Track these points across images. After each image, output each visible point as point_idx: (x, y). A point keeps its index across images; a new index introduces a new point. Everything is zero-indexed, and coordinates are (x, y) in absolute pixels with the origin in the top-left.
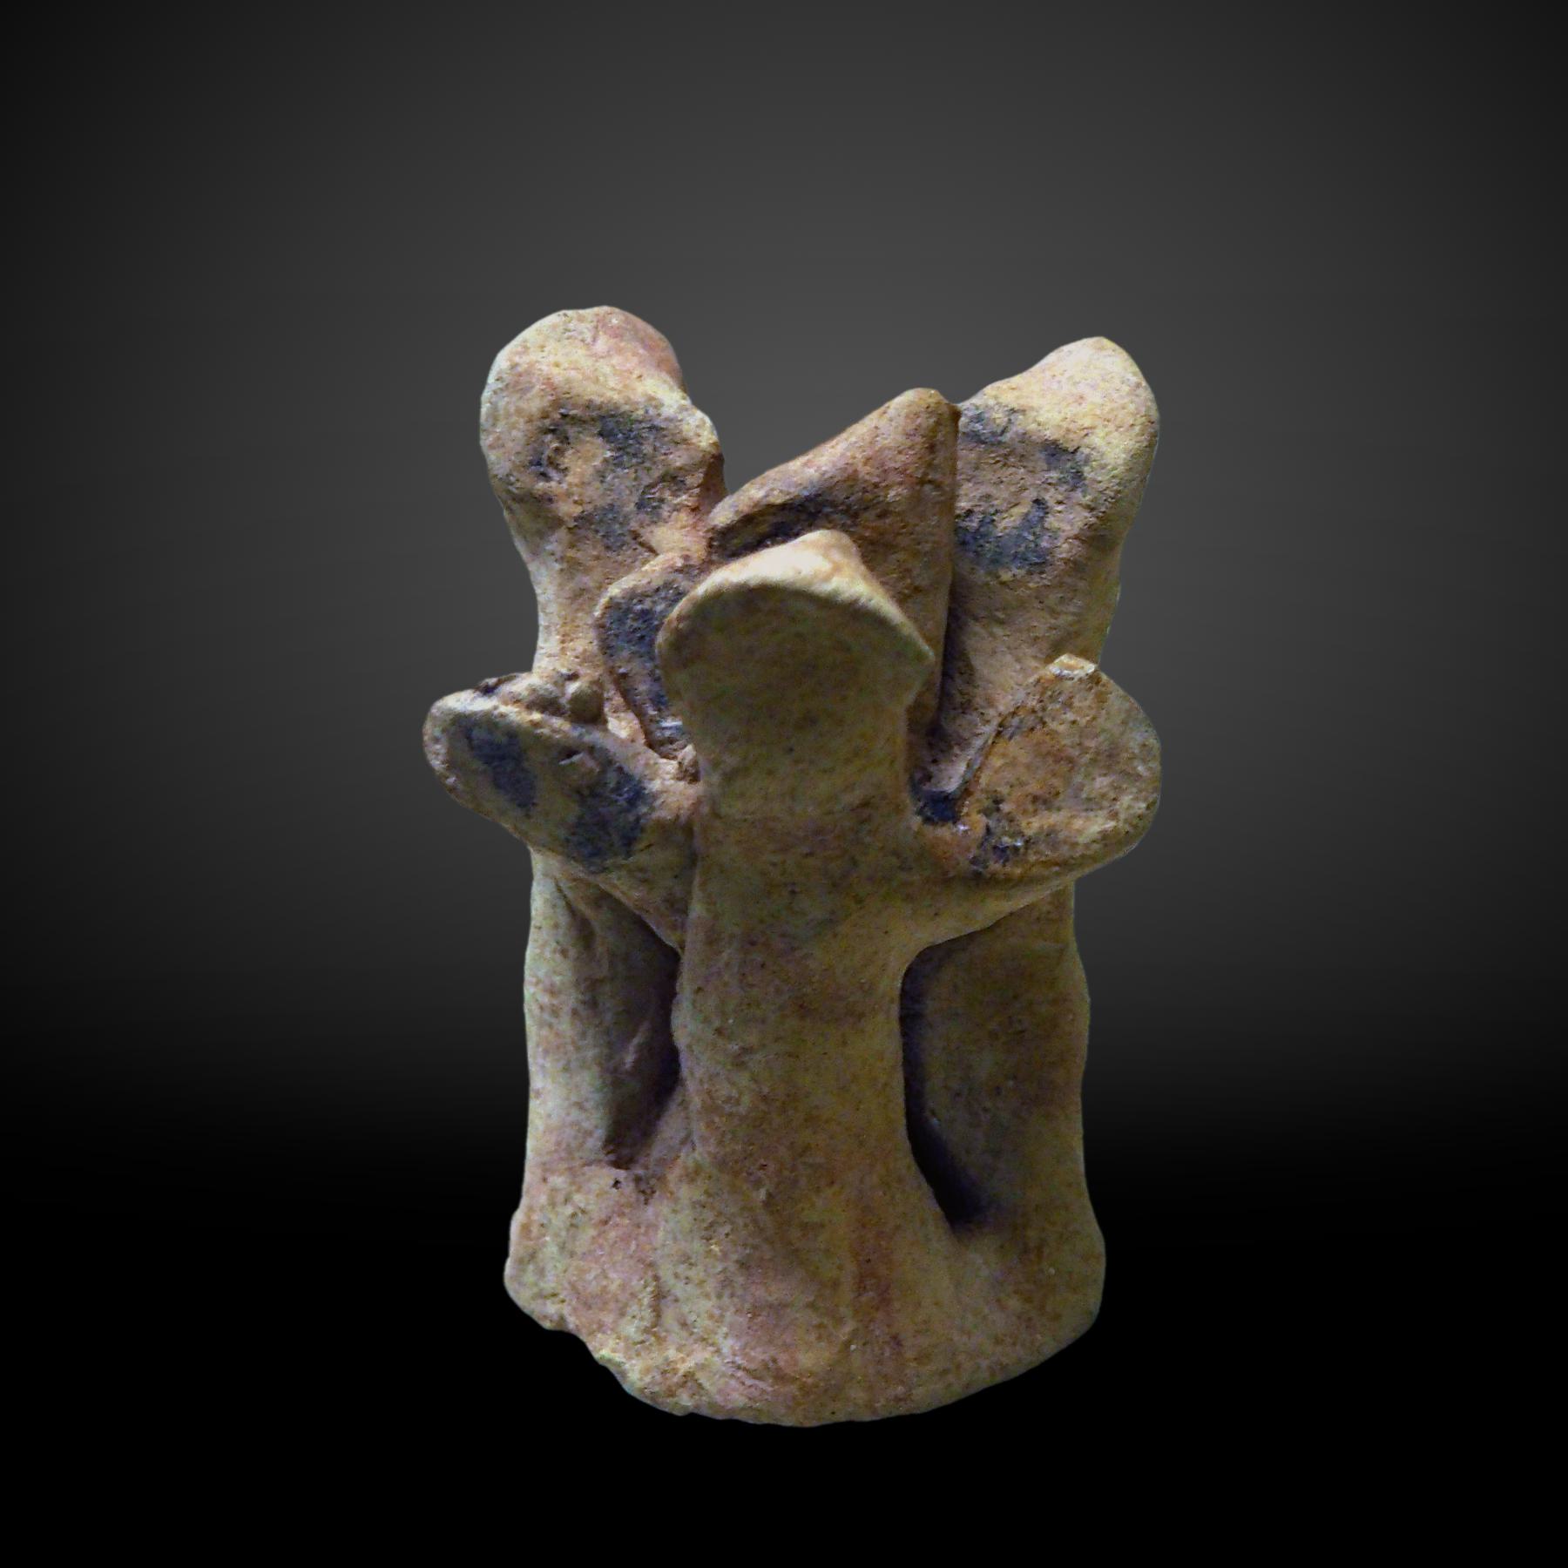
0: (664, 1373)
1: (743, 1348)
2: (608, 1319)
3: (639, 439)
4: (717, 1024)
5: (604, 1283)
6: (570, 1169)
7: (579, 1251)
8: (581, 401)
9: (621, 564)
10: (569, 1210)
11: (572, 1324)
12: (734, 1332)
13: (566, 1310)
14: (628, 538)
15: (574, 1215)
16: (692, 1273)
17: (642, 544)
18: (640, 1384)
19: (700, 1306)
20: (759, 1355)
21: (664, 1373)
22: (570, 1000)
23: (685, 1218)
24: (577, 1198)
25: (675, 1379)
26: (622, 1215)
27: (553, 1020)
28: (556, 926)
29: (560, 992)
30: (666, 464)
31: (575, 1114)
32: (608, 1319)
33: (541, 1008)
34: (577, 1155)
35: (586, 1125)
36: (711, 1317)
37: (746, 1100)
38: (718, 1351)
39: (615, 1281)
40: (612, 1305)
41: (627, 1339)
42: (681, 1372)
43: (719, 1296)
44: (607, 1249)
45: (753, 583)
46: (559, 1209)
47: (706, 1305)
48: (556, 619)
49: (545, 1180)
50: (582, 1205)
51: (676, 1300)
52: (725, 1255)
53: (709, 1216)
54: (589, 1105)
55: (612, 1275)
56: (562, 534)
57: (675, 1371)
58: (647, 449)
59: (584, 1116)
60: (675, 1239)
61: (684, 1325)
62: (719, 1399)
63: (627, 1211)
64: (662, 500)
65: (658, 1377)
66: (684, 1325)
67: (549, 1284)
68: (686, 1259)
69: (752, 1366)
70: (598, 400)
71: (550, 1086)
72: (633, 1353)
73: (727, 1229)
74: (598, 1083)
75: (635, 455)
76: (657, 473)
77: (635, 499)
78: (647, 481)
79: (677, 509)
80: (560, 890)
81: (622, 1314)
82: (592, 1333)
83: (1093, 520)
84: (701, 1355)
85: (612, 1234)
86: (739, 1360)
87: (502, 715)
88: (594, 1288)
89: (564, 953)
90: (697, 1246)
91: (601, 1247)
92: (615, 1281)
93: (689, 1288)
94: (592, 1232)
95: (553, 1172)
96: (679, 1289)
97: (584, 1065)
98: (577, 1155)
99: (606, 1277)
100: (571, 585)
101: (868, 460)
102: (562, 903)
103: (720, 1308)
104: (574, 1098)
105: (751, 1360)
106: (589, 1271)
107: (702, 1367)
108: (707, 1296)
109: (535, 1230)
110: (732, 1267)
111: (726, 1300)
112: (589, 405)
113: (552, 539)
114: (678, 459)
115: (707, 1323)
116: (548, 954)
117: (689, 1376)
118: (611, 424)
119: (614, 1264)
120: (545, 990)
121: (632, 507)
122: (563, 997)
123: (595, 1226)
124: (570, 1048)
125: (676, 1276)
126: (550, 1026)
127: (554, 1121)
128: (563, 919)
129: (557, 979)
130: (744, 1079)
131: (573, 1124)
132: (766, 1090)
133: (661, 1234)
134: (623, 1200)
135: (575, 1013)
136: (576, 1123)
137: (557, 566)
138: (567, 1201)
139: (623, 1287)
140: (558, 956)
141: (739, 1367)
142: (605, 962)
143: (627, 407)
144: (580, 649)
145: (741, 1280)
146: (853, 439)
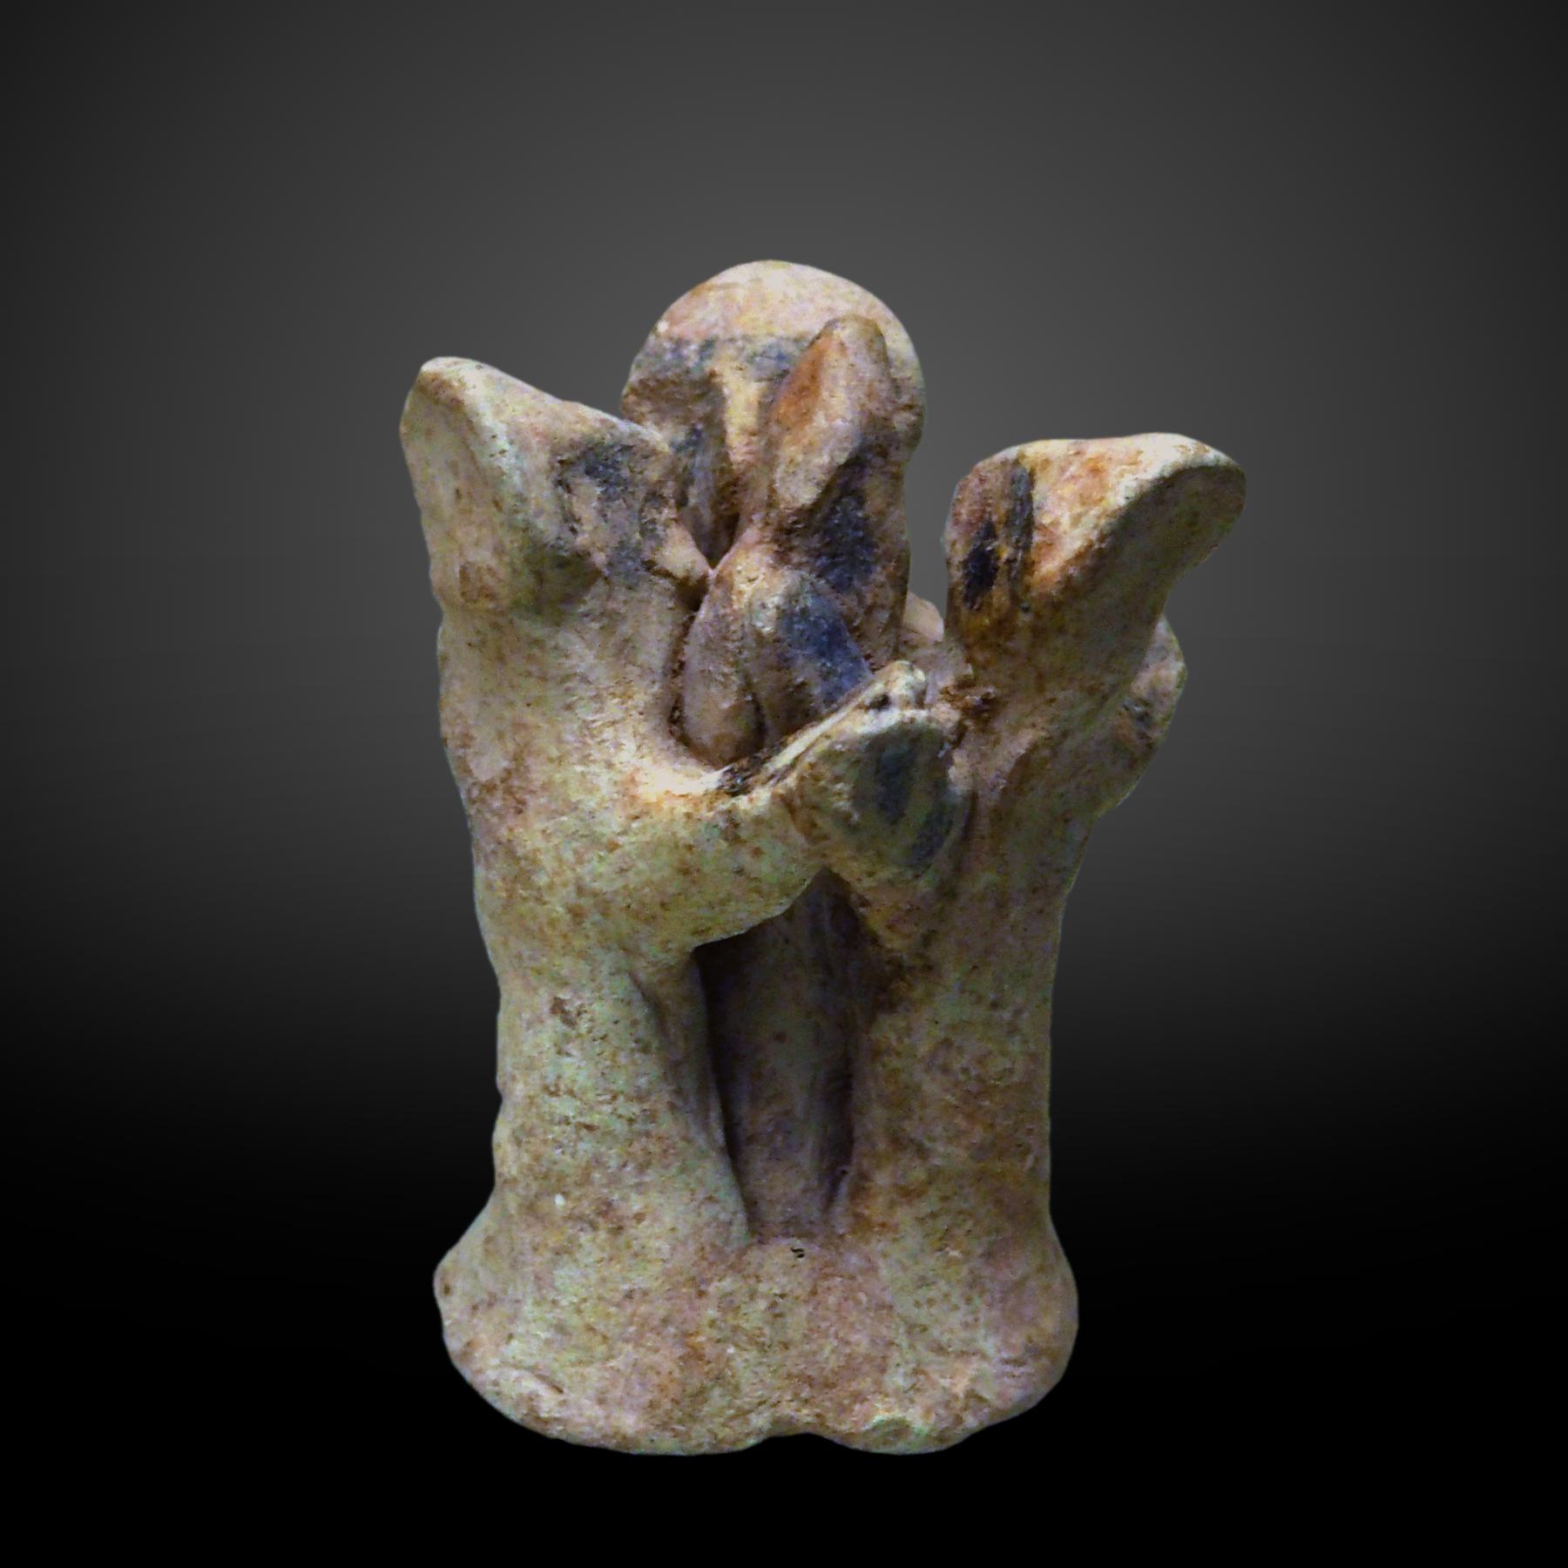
0: (947, 1405)
1: (1005, 1342)
2: (865, 1384)
3: (615, 465)
4: (992, 996)
5: (848, 1351)
6: (732, 1267)
7: (797, 1336)
8: (566, 443)
9: (641, 601)
10: (762, 1305)
11: (805, 1417)
12: (994, 1328)
13: (787, 1410)
14: (642, 572)
15: (773, 1305)
16: (933, 1293)
17: (655, 573)
18: (926, 1429)
19: (950, 1325)
20: (1018, 1339)
21: (947, 1405)
22: (662, 1098)
23: (912, 1238)
24: (763, 1287)
25: (959, 1405)
26: (826, 1277)
27: (651, 1127)
28: (634, 1023)
29: (649, 1093)
30: (646, 483)
31: (708, 1212)
32: (865, 1384)
33: (631, 1121)
34: (728, 1250)
35: (723, 1217)
36: (966, 1325)
37: (1019, 1067)
38: (984, 1357)
39: (861, 1342)
40: (866, 1368)
41: (897, 1392)
42: (961, 1395)
43: (969, 1301)
44: (834, 1318)
45: (1166, 474)
46: (744, 1309)
47: (955, 1319)
48: (605, 683)
49: (701, 1294)
50: (778, 1292)
51: (924, 1329)
52: (967, 1254)
53: (942, 1223)
54: (721, 1195)
55: (854, 1338)
56: (600, 588)
57: (956, 1397)
58: (625, 473)
59: (717, 1208)
60: (905, 1269)
61: (940, 1349)
62: (998, 1403)
63: (827, 1270)
64: (653, 521)
65: (941, 1411)
66: (940, 1349)
67: (751, 1393)
68: (923, 1282)
69: (1013, 1355)
70: (577, 437)
71: (655, 1198)
72: (906, 1402)
73: (969, 1225)
74: (721, 1166)
75: (618, 484)
76: (641, 494)
77: (637, 528)
78: (637, 506)
79: (666, 526)
80: (636, 982)
81: (883, 1371)
82: (843, 1410)
83: (913, 418)
84: (974, 1366)
85: (832, 1300)
86: (1005, 1355)
87: (912, 720)
88: (833, 1363)
89: (645, 1050)
90: (931, 1262)
91: (825, 1319)
92: (861, 1342)
93: (934, 1310)
94: (804, 1311)
95: (709, 1281)
96: (922, 1315)
97: (703, 1155)
98: (728, 1250)
99: (848, 1343)
100: (613, 640)
101: (869, 395)
102: (637, 996)
103: (973, 1312)
104: (701, 1196)
105: (1012, 1347)
106: (821, 1348)
107: (974, 1380)
108: (957, 1308)
109: (710, 1351)
110: (976, 1263)
111: (977, 1301)
112: (573, 445)
113: (587, 598)
114: (653, 473)
115: (964, 1335)
116: (622, 1059)
117: (971, 1395)
118: (591, 457)
119: (852, 1326)
120: (629, 1099)
121: (638, 536)
122: (653, 1098)
123: (806, 1302)
124: (681, 1144)
125: (917, 1304)
126: (647, 1134)
127: (683, 1230)
128: (641, 1012)
129: (643, 1081)
130: (1015, 1046)
131: (708, 1225)
132: (1033, 1047)
133: (884, 1272)
134: (816, 1264)
135: (672, 1107)
136: (715, 1218)
137: (595, 626)
138: (753, 1295)
139: (873, 1342)
140: (637, 1056)
141: (1007, 1362)
142: (681, 1044)
143: (597, 436)
144: (642, 704)
145: (987, 1272)
146: (843, 382)
